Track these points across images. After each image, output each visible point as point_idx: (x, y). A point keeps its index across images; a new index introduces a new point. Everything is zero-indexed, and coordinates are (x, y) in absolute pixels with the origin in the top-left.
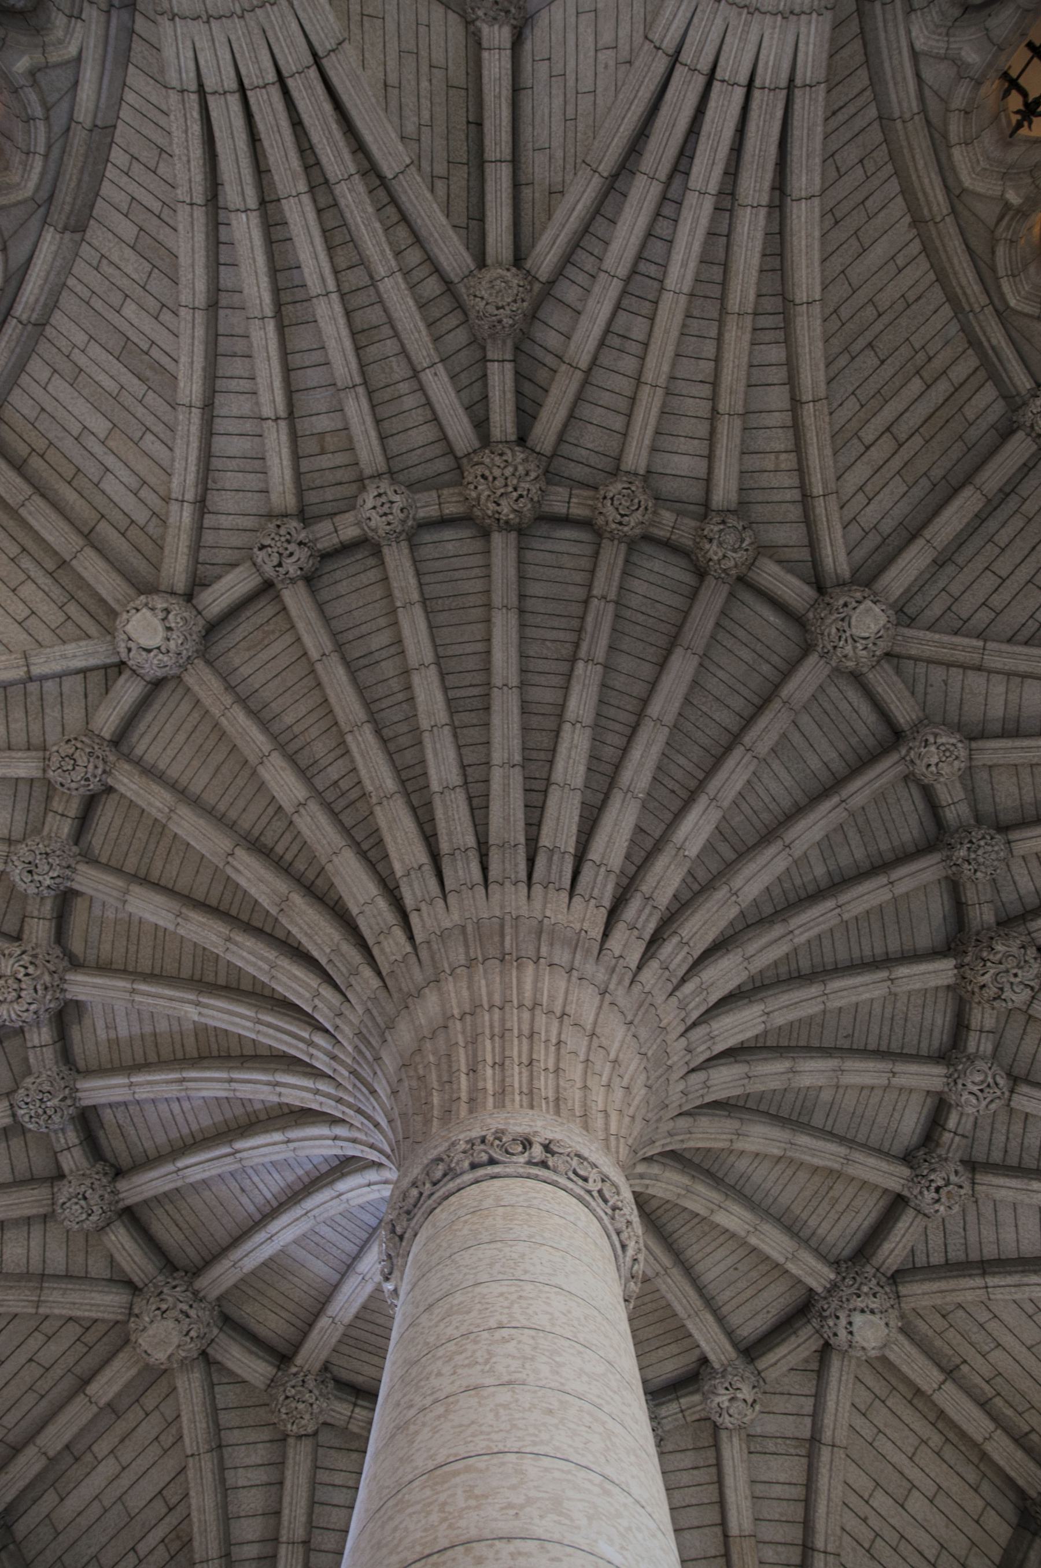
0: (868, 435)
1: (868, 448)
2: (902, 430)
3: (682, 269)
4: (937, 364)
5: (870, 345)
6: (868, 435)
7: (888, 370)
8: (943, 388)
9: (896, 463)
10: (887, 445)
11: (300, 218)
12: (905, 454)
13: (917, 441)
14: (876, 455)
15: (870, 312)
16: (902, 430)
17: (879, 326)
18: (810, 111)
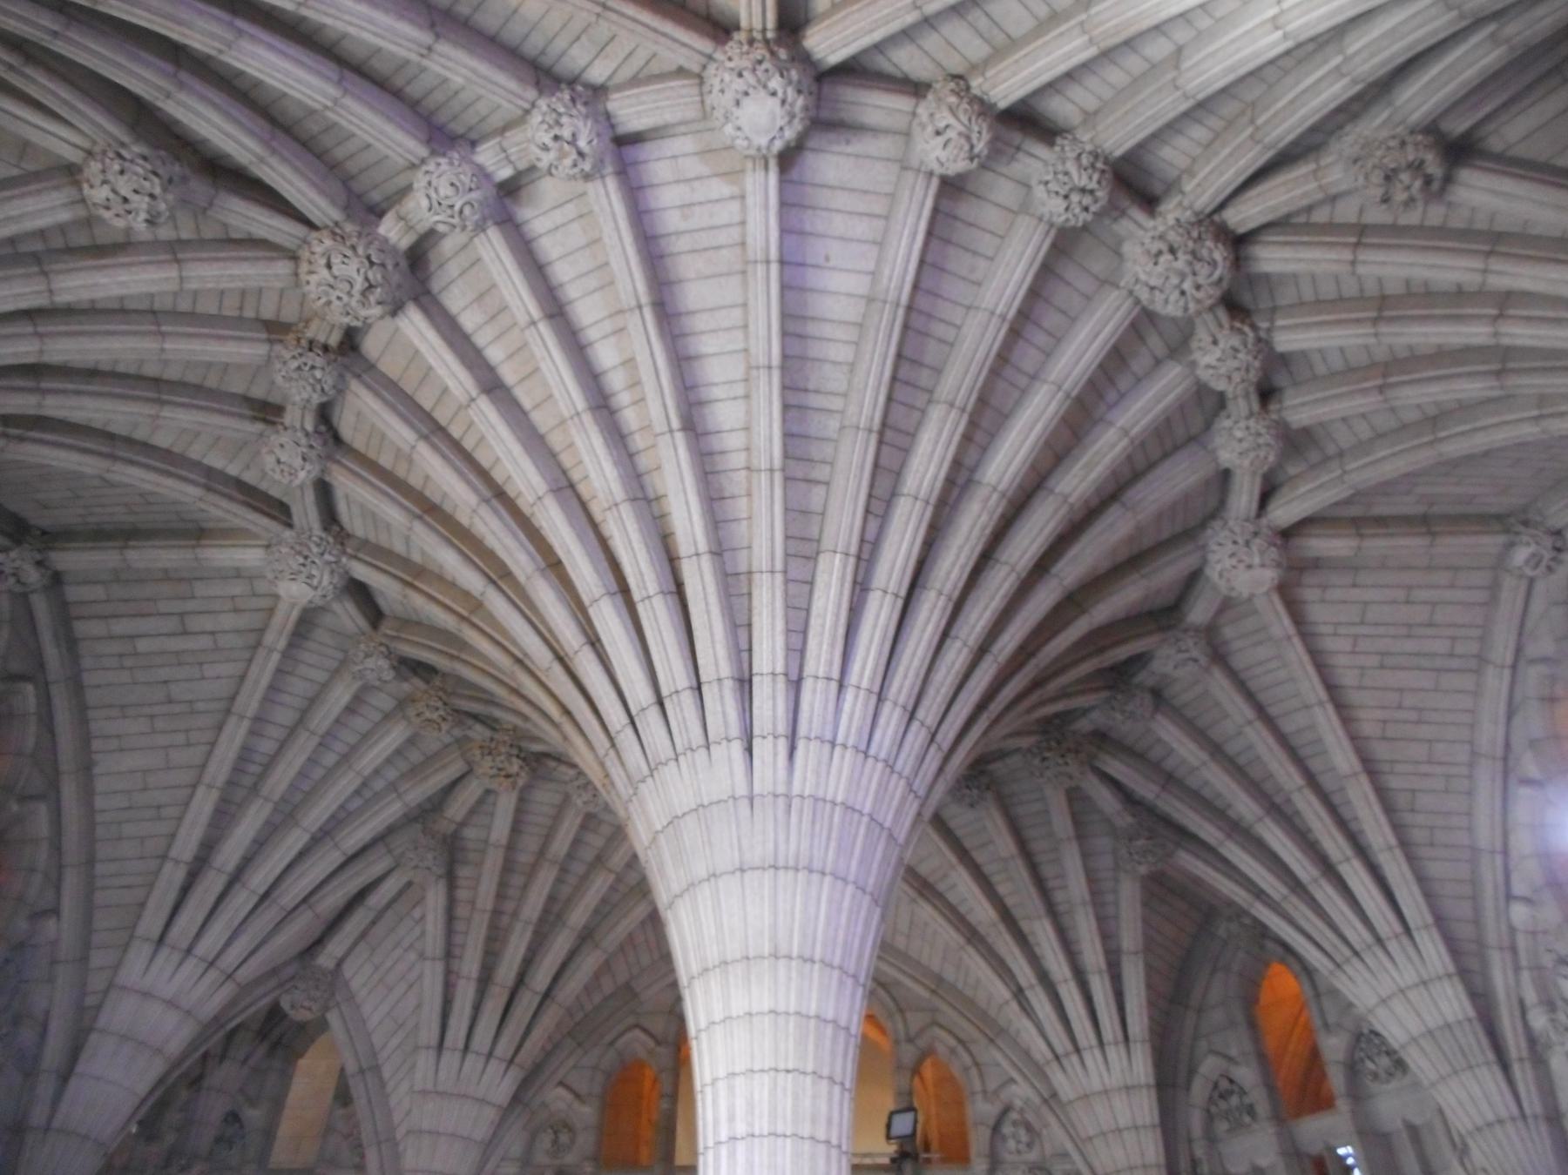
0: (205, 642)
1: (213, 633)
2: (171, 624)
3: (295, 840)
4: (116, 647)
5: (170, 702)
6: (205, 642)
7: (163, 674)
8: (120, 627)
9: (190, 605)
10: (194, 623)
11: (506, 972)
12: (177, 607)
13: (163, 607)
14: (207, 623)
15: (160, 724)
16: (171, 624)
17: (157, 710)
18: (152, 923)
